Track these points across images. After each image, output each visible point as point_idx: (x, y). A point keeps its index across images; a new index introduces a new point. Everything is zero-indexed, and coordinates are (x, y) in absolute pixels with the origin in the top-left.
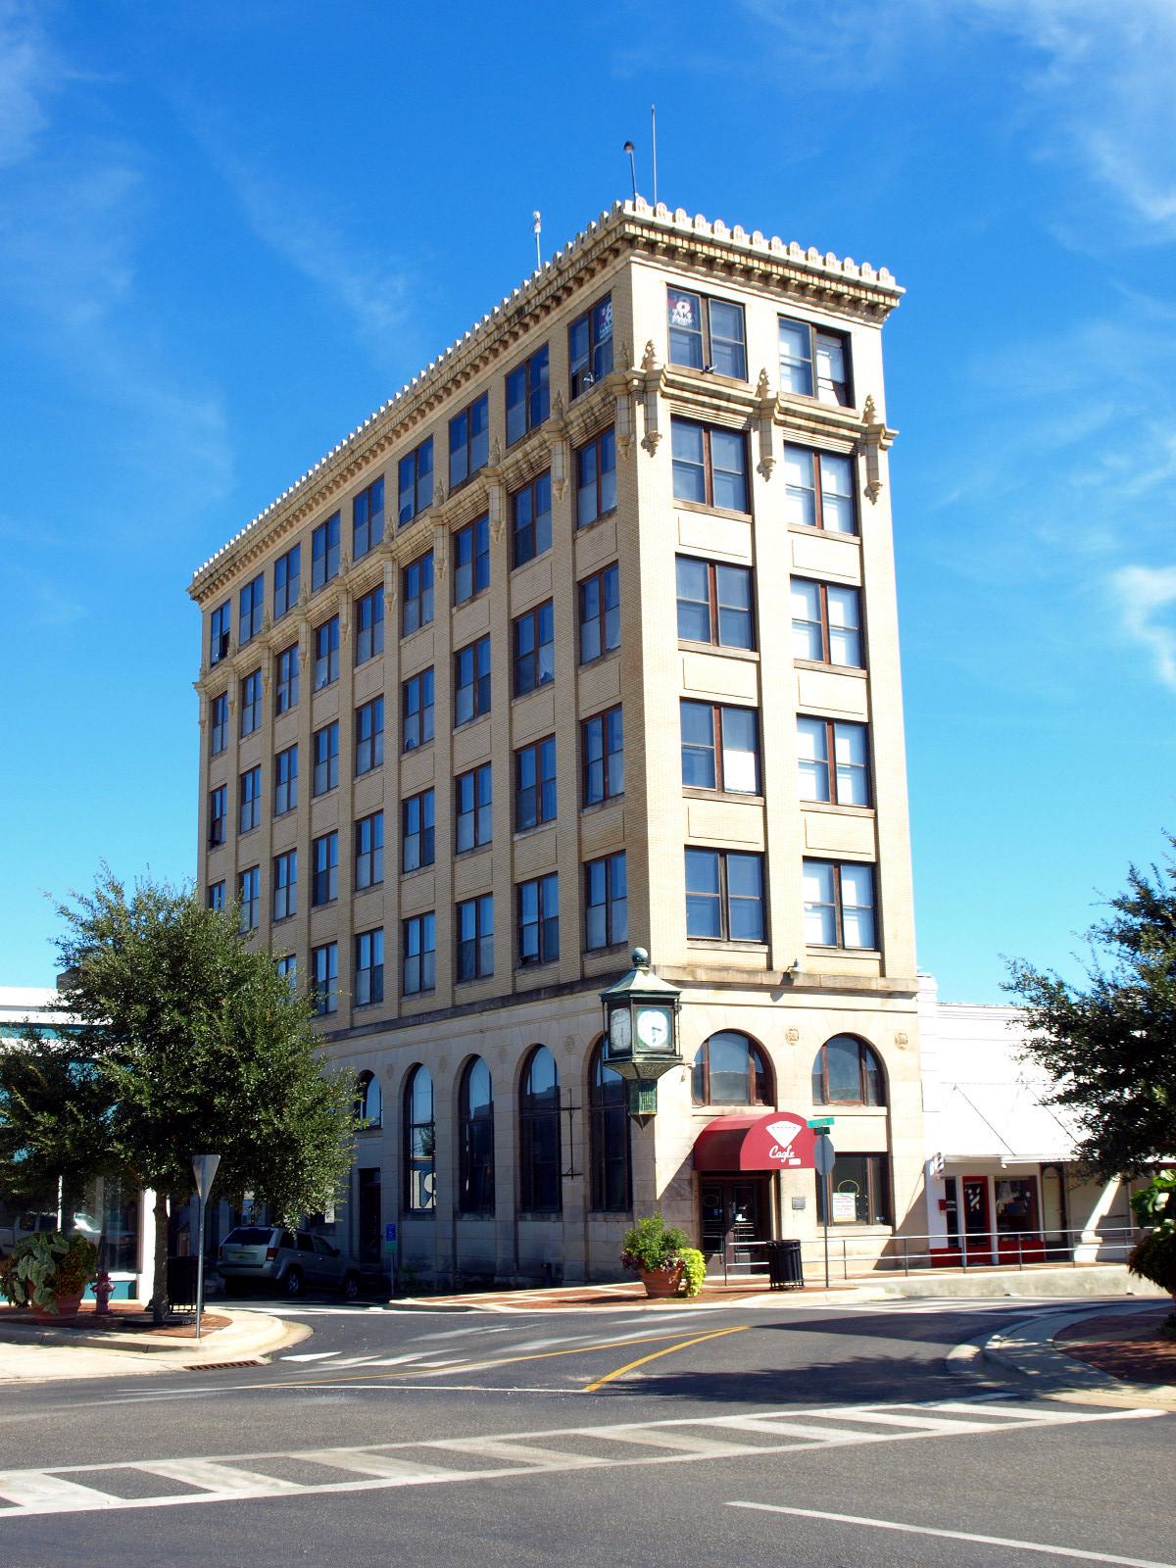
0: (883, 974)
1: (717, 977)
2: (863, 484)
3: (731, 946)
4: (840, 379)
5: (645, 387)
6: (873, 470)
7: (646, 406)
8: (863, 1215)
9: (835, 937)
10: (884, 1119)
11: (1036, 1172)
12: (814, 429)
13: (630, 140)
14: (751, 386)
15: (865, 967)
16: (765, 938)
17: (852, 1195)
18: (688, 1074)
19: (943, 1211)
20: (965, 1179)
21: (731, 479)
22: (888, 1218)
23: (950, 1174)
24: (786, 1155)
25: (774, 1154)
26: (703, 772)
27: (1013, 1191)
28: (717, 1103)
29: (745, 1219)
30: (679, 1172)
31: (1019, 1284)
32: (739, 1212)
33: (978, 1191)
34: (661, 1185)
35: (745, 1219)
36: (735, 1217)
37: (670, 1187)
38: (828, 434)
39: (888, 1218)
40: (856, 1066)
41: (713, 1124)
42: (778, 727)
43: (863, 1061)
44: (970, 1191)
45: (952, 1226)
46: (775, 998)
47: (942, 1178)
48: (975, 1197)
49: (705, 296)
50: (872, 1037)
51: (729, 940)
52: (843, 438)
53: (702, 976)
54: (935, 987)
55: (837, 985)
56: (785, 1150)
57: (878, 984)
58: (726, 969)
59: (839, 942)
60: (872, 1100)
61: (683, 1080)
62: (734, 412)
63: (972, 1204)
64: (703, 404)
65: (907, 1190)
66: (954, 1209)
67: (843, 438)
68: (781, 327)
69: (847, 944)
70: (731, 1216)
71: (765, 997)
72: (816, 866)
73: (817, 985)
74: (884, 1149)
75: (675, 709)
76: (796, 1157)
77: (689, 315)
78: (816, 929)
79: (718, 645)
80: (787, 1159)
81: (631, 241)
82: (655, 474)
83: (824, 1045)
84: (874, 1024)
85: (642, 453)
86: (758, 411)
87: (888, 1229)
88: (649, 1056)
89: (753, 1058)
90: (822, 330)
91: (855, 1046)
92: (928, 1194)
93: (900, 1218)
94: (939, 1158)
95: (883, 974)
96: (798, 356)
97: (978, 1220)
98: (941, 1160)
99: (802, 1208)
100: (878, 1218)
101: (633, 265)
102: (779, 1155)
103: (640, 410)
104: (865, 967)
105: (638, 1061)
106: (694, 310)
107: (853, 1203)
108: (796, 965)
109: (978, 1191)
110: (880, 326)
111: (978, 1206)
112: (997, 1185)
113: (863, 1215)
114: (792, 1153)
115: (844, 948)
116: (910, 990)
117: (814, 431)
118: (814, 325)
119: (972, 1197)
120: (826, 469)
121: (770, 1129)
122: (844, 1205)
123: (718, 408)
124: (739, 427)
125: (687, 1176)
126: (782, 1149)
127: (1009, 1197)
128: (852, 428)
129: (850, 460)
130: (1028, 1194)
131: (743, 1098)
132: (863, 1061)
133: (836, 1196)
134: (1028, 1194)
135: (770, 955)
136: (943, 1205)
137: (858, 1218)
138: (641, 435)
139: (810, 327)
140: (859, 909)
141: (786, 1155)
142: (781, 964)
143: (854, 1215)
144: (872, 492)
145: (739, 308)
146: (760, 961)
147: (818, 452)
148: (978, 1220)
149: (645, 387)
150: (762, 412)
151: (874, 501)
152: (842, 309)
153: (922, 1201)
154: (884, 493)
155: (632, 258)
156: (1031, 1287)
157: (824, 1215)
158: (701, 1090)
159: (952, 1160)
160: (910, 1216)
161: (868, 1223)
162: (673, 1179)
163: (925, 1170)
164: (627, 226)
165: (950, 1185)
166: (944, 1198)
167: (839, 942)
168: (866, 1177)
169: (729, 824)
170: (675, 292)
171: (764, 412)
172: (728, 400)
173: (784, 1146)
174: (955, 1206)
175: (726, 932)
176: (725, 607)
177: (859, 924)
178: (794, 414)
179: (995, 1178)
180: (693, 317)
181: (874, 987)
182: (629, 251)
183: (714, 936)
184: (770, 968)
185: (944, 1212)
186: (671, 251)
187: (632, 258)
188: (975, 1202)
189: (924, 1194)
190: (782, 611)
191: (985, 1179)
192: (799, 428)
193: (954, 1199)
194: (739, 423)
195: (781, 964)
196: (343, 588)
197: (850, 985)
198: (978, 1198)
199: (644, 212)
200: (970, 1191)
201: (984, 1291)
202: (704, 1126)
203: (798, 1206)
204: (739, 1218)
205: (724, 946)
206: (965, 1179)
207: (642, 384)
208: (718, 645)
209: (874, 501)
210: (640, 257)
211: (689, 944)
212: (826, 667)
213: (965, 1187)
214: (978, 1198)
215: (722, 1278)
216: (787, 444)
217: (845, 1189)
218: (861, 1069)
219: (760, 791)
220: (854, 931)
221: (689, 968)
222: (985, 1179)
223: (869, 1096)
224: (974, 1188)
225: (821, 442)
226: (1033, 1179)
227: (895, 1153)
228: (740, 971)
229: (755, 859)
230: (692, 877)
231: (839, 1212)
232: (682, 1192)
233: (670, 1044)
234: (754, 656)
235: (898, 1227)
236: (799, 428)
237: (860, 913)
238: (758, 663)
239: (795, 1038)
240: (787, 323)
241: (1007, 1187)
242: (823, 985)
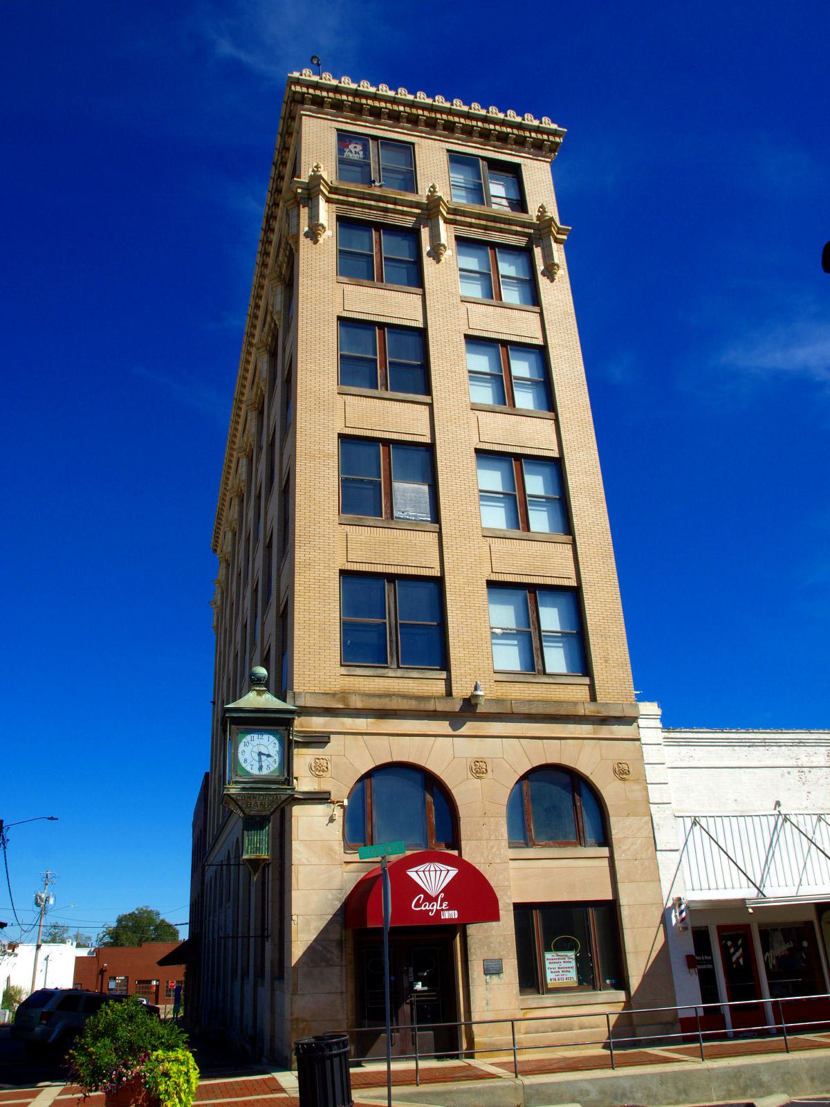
0: (593, 698)
2: (540, 267)
3: (400, 673)
4: (514, 196)
5: (309, 194)
6: (548, 255)
7: (310, 209)
8: (587, 979)
9: (533, 663)
10: (606, 863)
11: (812, 916)
12: (486, 226)
13: (315, 54)
14: (421, 196)
15: (576, 693)
16: (445, 665)
17: (572, 954)
18: (338, 813)
19: (692, 970)
20: (720, 928)
21: (404, 266)
22: (621, 982)
23: (700, 923)
24: (436, 906)
25: (418, 905)
26: (363, 496)
27: (786, 940)
29: (426, 988)
30: (325, 931)
31: (785, 1074)
32: (417, 979)
33: (740, 942)
34: (297, 950)
35: (426, 988)
36: (412, 985)
37: (311, 950)
38: (501, 231)
39: (621, 982)
40: (562, 804)
41: (369, 873)
42: (455, 465)
43: (577, 797)
44: (729, 943)
45: (709, 992)
46: (455, 726)
47: (685, 928)
48: (736, 951)
49: (375, 138)
50: (584, 767)
51: (398, 667)
52: (516, 233)
53: (357, 703)
54: (659, 712)
55: (533, 711)
56: (436, 899)
57: (588, 709)
58: (389, 695)
59: (540, 668)
60: (590, 838)
61: (332, 820)
62: (403, 213)
63: (734, 958)
64: (370, 207)
65: (641, 946)
66: (710, 966)
67: (516, 233)
68: (450, 161)
69: (548, 670)
70: (406, 984)
71: (443, 727)
72: (505, 593)
73: (509, 711)
74: (609, 897)
75: (333, 447)
76: (450, 908)
77: (361, 153)
78: (509, 657)
79: (387, 390)
80: (438, 912)
81: (300, 100)
82: (318, 260)
83: (526, 777)
84: (585, 753)
85: (304, 243)
86: (426, 212)
87: (621, 995)
89: (432, 796)
90: (495, 165)
91: (566, 779)
92: (671, 950)
93: (635, 981)
94: (680, 905)
95: (593, 698)
96: (471, 179)
97: (743, 982)
98: (683, 907)
99: (498, 972)
100: (608, 981)
101: (304, 117)
102: (426, 907)
103: (304, 212)
104: (576, 693)
105: (232, 791)
106: (366, 149)
107: (573, 964)
108: (476, 688)
109: (740, 942)
110: (549, 160)
111: (741, 961)
112: (765, 934)
113: (587, 979)
114: (445, 904)
115: (544, 673)
116: (627, 714)
117: (486, 228)
118: (484, 158)
119: (732, 950)
120: (504, 261)
121: (412, 874)
122: (559, 967)
123: (386, 210)
124: (410, 225)
125: (335, 936)
126: (429, 899)
127: (781, 948)
128: (524, 225)
129: (527, 252)
130: (805, 944)
131: (418, 842)
132: (577, 797)
133: (548, 955)
134: (805, 944)
135: (448, 682)
136: (691, 962)
137: (580, 982)
138: (305, 228)
139: (480, 161)
140: (564, 635)
141: (436, 906)
143: (575, 979)
144: (550, 272)
145: (409, 148)
146: (440, 688)
147: (494, 245)
148: (743, 982)
149: (309, 194)
150: (430, 211)
151: (552, 280)
152: (509, 146)
153: (662, 960)
154: (562, 273)
155: (302, 112)
156: (804, 1077)
157: (531, 979)
159: (693, 906)
160: (647, 977)
161: (594, 988)
162: (316, 940)
163: (665, 919)
164: (293, 87)
165: (700, 937)
166: (693, 953)
167: (539, 667)
168: (580, 932)
169: (397, 549)
170: (344, 138)
171: (431, 212)
172: (395, 204)
173: (433, 894)
174: (711, 962)
175: (395, 659)
176: (391, 359)
177: (565, 651)
178: (464, 214)
179: (760, 926)
180: (364, 154)
181: (581, 712)
182: (299, 106)
183: (378, 662)
184: (449, 693)
185: (694, 971)
186: (338, 106)
187: (302, 112)
188: (737, 955)
189: (665, 950)
190: (451, 364)
191: (747, 927)
192: (471, 225)
193: (709, 952)
194: (409, 222)
195: (461, 689)
196: (235, 494)
197: (551, 710)
198: (740, 951)
199: (308, 75)
200: (729, 943)
201: (732, 1087)
202: (363, 875)
203: (493, 969)
204: (419, 986)
205: (391, 673)
206: (720, 928)
207: (305, 192)
208: (387, 390)
209: (552, 280)
210: (310, 111)
211: (344, 671)
212: (509, 410)
213: (721, 938)
214: (740, 951)
215: (382, 1067)
216: (460, 240)
217: (562, 946)
218: (575, 804)
219: (436, 517)
220: (556, 659)
221: (344, 695)
222: (747, 927)
223: (587, 836)
224: (734, 939)
225: (496, 237)
226: (809, 924)
227: (623, 901)
229: (431, 585)
230: (350, 604)
231: (553, 976)
232: (329, 955)
233: (282, 773)
234: (427, 399)
235: (632, 992)
236: (471, 225)
237: (565, 639)
238: (431, 405)
239: (482, 770)
240: (456, 159)
241: (779, 936)
242: (515, 711)
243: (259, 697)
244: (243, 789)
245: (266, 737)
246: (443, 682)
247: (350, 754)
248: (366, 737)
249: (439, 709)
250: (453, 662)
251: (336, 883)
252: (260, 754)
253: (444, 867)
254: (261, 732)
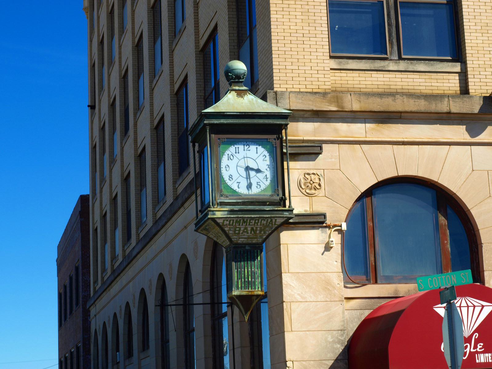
1: (376, 105)
3: (402, 65)
16: (458, 53)
18: (336, 239)
28: (389, 280)
41: (376, 311)
46: (473, 133)
51: (400, 58)
53: (354, 104)
58: (392, 94)
61: (328, 248)
71: (459, 132)
80: (472, 355)
88: (236, 208)
89: (446, 216)
105: (219, 215)
142: (479, 87)
146: (452, 83)
158: (360, 263)
175: (395, 48)
183: (375, 52)
184: (465, 90)
202: (367, 313)
205: (392, 66)
211: (333, 64)
221: (336, 94)
228: (411, 95)
233: (275, 191)
243: (240, 99)
244: (232, 212)
245: (253, 148)
246: (457, 77)
247: (342, 171)
248: (364, 147)
249: (454, 110)
250: (469, 51)
251: (337, 323)
252: (248, 169)
253: (477, 302)
254: (247, 142)
